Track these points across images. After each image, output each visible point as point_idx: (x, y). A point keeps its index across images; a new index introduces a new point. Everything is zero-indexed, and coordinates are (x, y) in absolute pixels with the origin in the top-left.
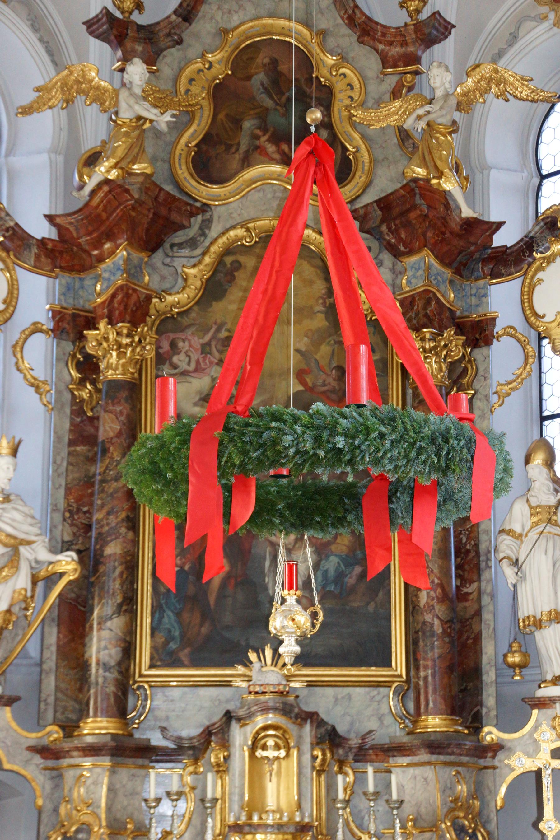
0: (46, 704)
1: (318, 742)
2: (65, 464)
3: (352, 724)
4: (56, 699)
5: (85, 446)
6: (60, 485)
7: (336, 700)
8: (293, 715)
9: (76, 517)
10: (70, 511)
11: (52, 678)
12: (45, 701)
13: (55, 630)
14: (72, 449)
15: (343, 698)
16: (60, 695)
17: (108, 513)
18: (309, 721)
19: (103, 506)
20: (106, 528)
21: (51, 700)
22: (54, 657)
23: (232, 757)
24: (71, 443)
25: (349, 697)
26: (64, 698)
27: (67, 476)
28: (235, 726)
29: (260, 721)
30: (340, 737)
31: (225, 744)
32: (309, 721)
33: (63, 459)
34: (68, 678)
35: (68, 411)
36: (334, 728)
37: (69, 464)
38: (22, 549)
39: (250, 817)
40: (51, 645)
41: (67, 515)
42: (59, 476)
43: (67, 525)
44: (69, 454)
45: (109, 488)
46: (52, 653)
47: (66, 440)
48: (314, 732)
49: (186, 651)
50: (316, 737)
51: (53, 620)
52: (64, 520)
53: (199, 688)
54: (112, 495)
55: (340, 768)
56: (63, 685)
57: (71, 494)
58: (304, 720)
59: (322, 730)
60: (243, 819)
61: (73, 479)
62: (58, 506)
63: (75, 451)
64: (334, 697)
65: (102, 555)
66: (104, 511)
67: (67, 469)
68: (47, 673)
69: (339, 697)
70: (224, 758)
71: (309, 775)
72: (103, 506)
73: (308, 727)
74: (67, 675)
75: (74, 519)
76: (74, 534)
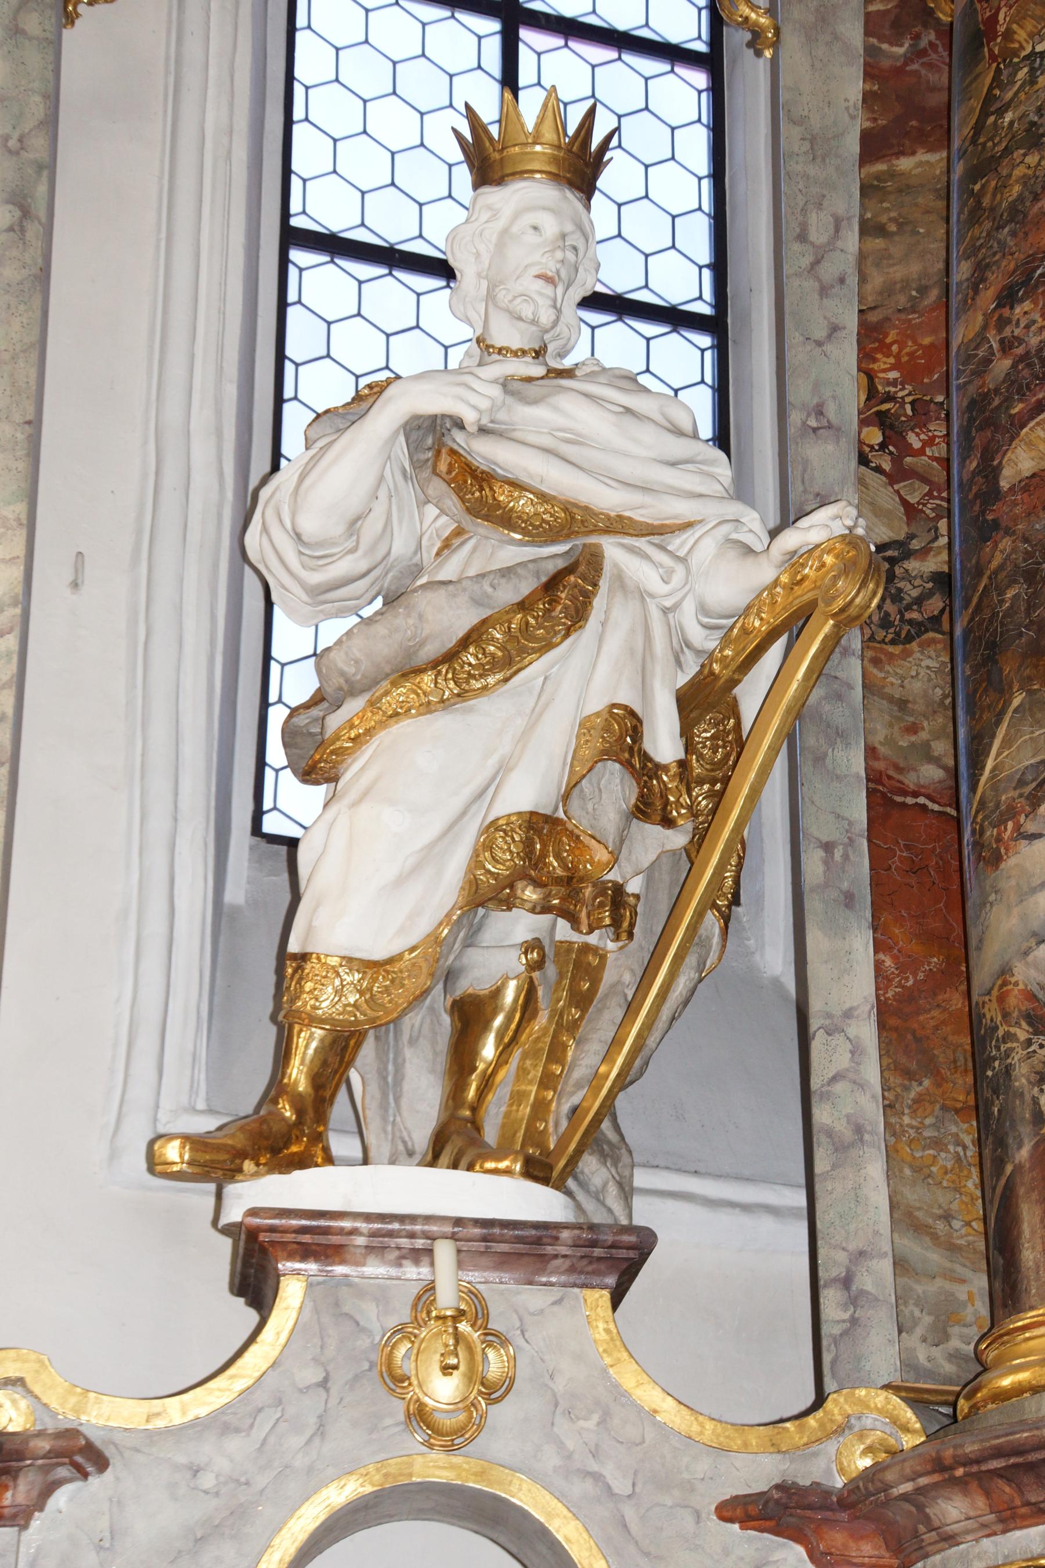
0: (854, 1300)
2: (851, 240)
4: (900, 1265)
5: (931, 149)
6: (834, 329)
9: (915, 441)
10: (882, 420)
11: (875, 1169)
12: (846, 1282)
13: (861, 944)
14: (881, 167)
16: (915, 1248)
17: (1008, 297)
19: (976, 283)
20: (1002, 365)
21: (878, 1276)
22: (872, 1071)
24: (873, 146)
26: (935, 1257)
27: (863, 279)
33: (838, 224)
34: (946, 1160)
35: (854, 33)
37: (868, 229)
38: (614, 551)
40: (848, 1014)
41: (875, 436)
42: (824, 291)
43: (875, 480)
44: (867, 190)
45: (1003, 185)
46: (856, 1051)
47: (852, 145)
51: (849, 900)
52: (863, 460)
54: (1016, 213)
56: (912, 1195)
57: (885, 348)
61: (888, 290)
62: (831, 411)
63: (892, 174)
65: (992, 494)
66: (987, 297)
67: (862, 257)
68: (841, 1148)
72: (976, 283)
74: (938, 1144)
75: (907, 450)
76: (911, 511)
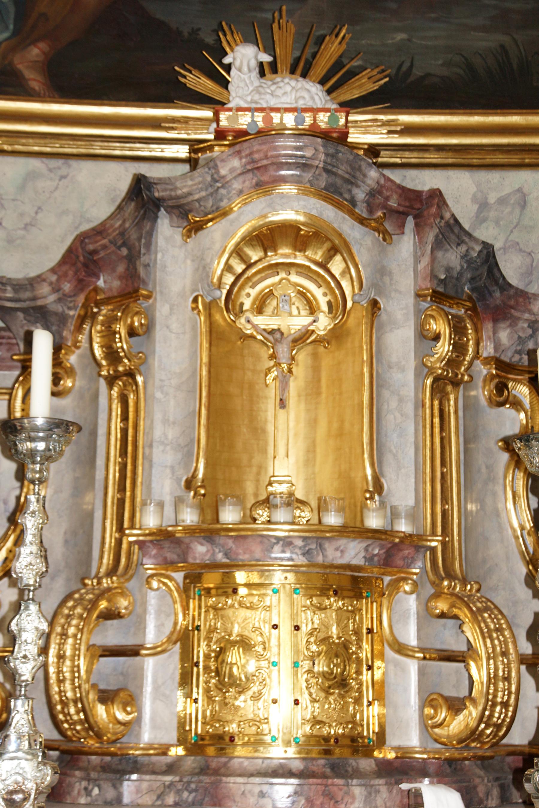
1: (440, 294)
3: (528, 273)
7: (484, 205)
8: (360, 195)
15: (502, 201)
18: (410, 222)
23: (159, 333)
25: (522, 200)
28: (166, 230)
29: (247, 216)
30: (505, 286)
31: (133, 291)
32: (410, 222)
36: (488, 254)
39: (210, 507)
48: (425, 261)
49: (35, 52)
50: (433, 276)
53: (74, 163)
55: (501, 387)
58: (400, 216)
59: (452, 258)
60: (190, 517)
64: (474, 199)
69: (492, 198)
70: (132, 333)
71: (409, 391)
73: (406, 245)
